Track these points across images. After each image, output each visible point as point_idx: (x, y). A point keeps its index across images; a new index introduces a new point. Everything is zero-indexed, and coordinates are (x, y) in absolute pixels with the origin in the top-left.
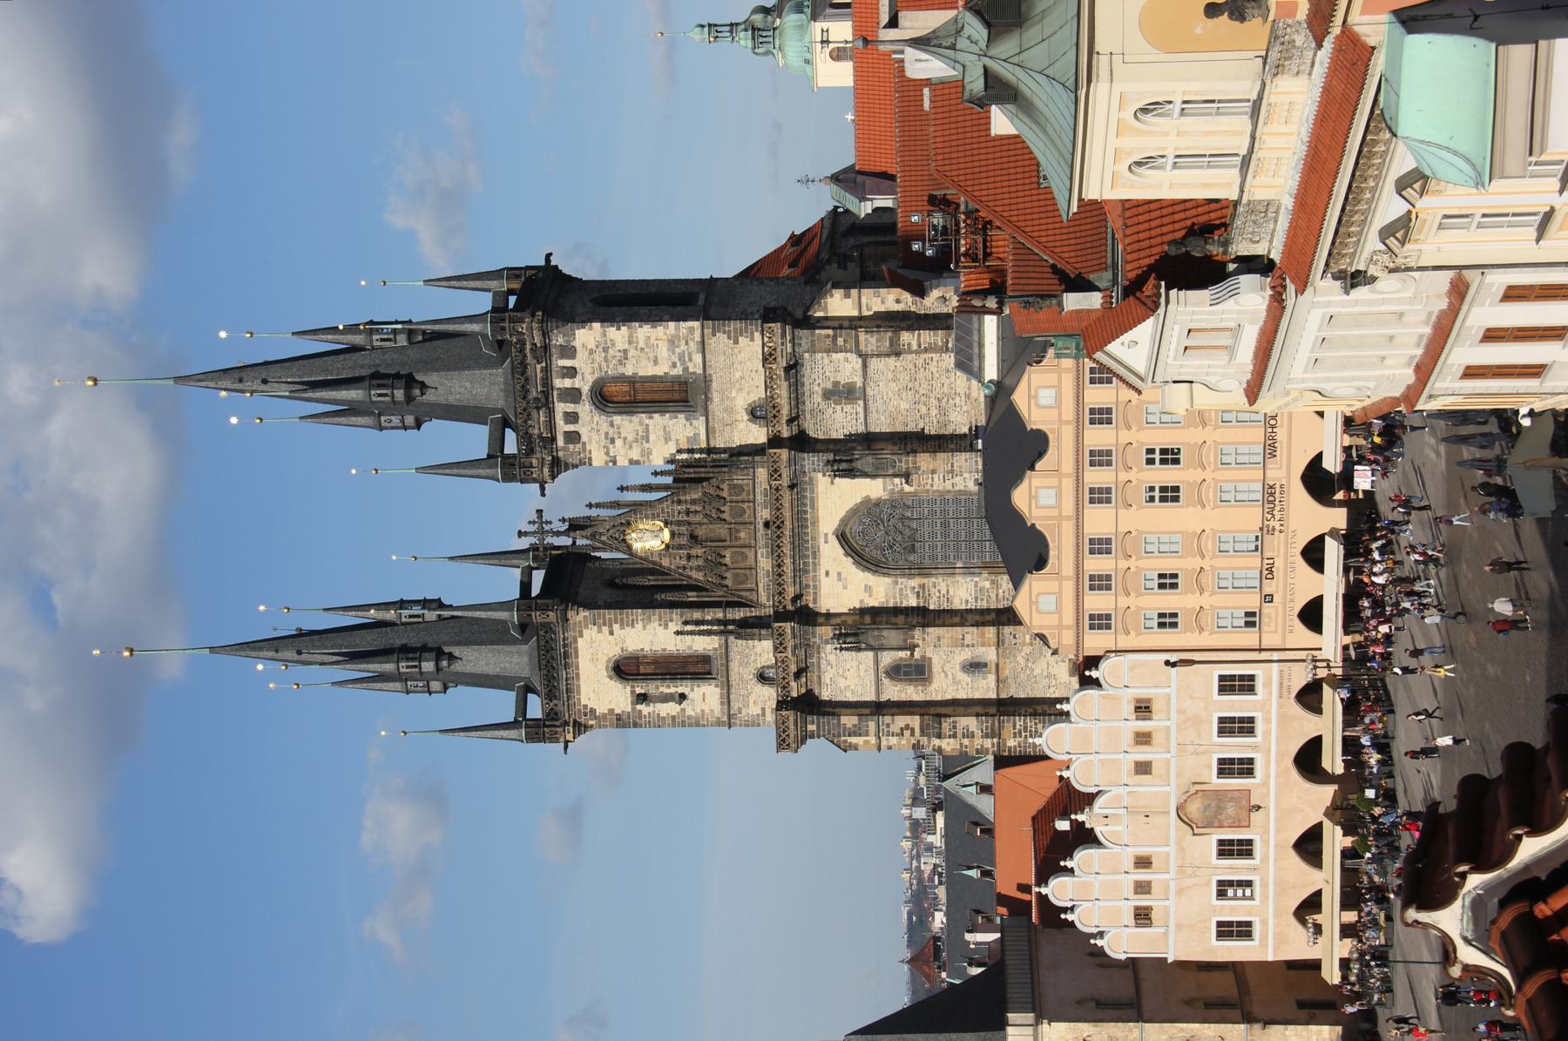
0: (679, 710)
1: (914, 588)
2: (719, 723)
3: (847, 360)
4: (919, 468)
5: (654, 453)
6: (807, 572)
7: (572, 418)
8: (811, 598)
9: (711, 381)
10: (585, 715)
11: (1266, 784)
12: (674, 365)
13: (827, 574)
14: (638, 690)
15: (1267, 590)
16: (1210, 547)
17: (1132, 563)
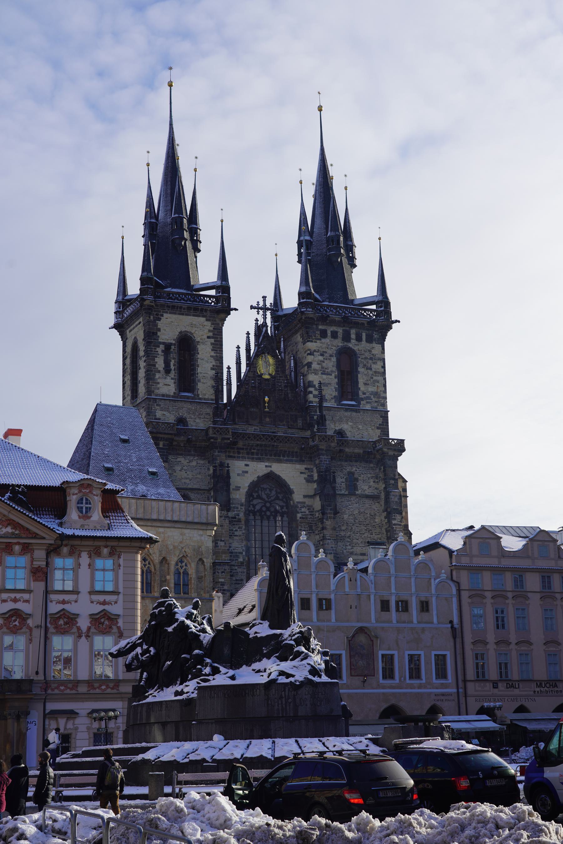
0: (159, 369)
1: (239, 516)
2: (149, 391)
3: (370, 487)
4: (327, 520)
5: (315, 376)
6: (248, 453)
7: (334, 335)
8: (232, 454)
9: (356, 412)
10: (157, 315)
11: (379, 686)
12: (364, 394)
13: (247, 465)
14: (173, 347)
15: (500, 685)
16: (522, 648)
17: (510, 601)
